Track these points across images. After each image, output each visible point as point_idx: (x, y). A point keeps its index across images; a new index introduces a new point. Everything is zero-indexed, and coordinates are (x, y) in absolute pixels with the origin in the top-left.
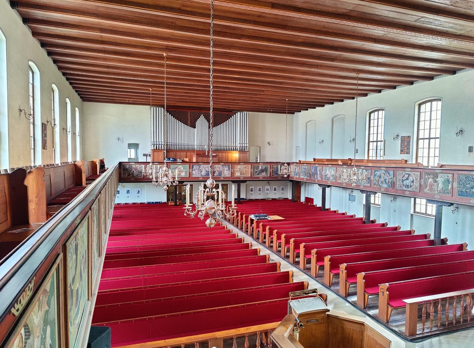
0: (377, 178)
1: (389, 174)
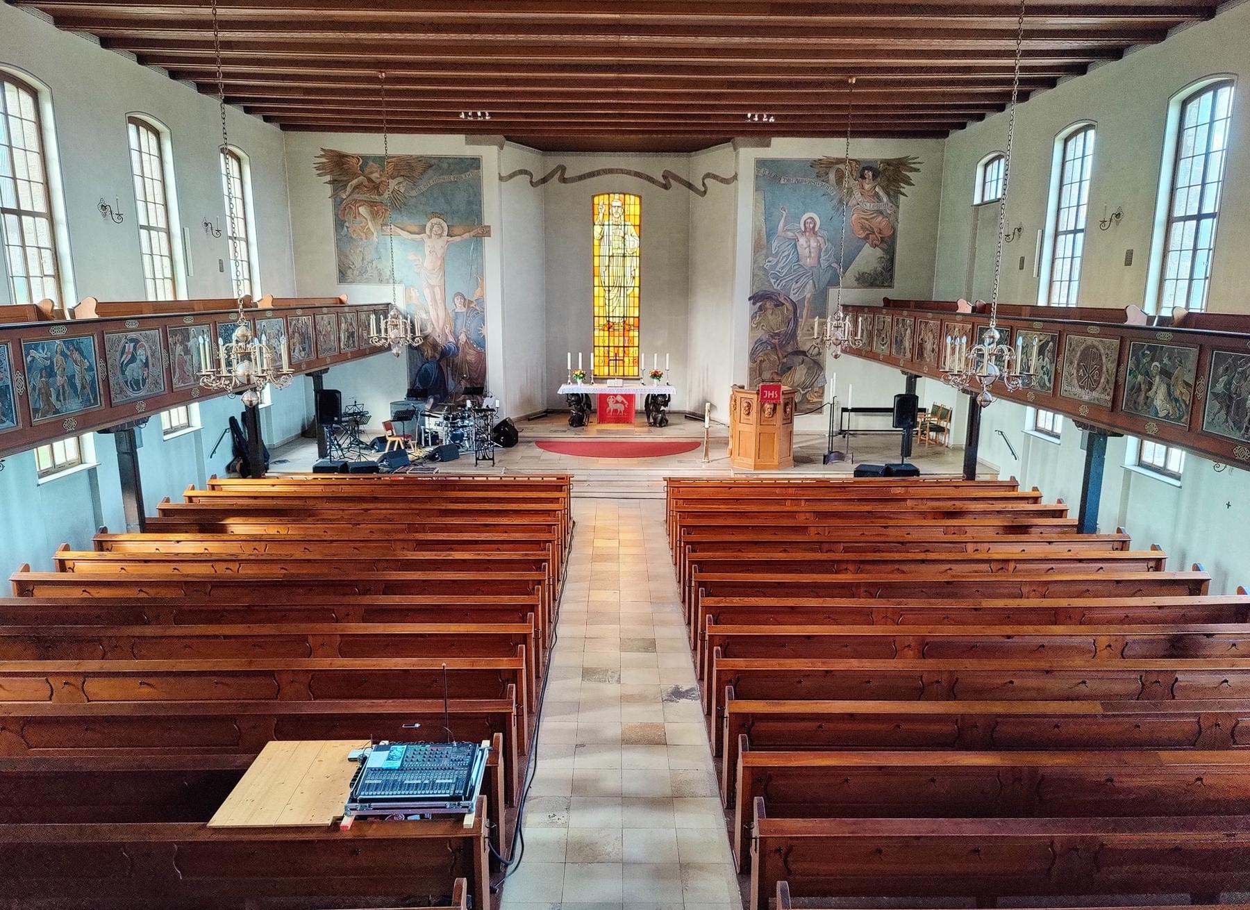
0: (37, 381)
1: (81, 353)
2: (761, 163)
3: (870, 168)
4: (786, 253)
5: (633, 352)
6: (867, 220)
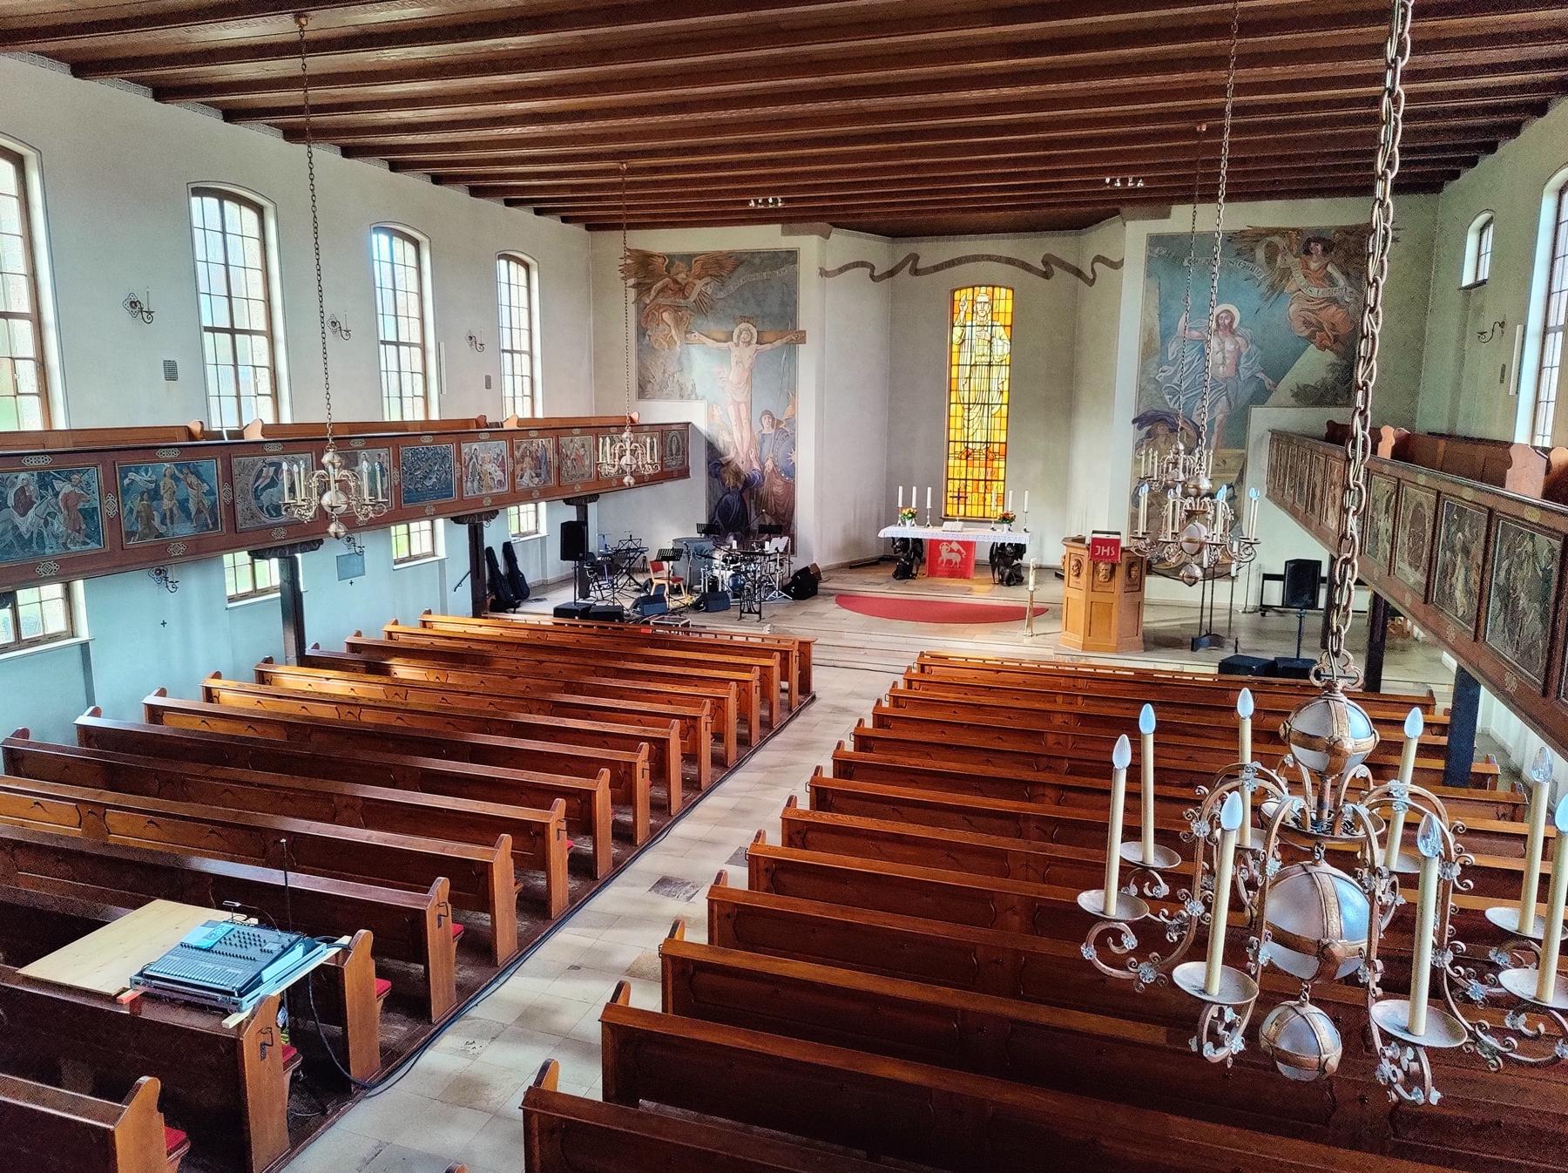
0: (137, 504)
1: (198, 475)
2: (1155, 241)
3: (1318, 240)
4: (1189, 359)
5: (997, 487)
6: (1313, 312)
